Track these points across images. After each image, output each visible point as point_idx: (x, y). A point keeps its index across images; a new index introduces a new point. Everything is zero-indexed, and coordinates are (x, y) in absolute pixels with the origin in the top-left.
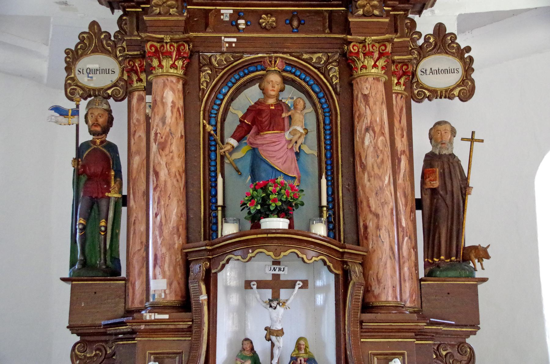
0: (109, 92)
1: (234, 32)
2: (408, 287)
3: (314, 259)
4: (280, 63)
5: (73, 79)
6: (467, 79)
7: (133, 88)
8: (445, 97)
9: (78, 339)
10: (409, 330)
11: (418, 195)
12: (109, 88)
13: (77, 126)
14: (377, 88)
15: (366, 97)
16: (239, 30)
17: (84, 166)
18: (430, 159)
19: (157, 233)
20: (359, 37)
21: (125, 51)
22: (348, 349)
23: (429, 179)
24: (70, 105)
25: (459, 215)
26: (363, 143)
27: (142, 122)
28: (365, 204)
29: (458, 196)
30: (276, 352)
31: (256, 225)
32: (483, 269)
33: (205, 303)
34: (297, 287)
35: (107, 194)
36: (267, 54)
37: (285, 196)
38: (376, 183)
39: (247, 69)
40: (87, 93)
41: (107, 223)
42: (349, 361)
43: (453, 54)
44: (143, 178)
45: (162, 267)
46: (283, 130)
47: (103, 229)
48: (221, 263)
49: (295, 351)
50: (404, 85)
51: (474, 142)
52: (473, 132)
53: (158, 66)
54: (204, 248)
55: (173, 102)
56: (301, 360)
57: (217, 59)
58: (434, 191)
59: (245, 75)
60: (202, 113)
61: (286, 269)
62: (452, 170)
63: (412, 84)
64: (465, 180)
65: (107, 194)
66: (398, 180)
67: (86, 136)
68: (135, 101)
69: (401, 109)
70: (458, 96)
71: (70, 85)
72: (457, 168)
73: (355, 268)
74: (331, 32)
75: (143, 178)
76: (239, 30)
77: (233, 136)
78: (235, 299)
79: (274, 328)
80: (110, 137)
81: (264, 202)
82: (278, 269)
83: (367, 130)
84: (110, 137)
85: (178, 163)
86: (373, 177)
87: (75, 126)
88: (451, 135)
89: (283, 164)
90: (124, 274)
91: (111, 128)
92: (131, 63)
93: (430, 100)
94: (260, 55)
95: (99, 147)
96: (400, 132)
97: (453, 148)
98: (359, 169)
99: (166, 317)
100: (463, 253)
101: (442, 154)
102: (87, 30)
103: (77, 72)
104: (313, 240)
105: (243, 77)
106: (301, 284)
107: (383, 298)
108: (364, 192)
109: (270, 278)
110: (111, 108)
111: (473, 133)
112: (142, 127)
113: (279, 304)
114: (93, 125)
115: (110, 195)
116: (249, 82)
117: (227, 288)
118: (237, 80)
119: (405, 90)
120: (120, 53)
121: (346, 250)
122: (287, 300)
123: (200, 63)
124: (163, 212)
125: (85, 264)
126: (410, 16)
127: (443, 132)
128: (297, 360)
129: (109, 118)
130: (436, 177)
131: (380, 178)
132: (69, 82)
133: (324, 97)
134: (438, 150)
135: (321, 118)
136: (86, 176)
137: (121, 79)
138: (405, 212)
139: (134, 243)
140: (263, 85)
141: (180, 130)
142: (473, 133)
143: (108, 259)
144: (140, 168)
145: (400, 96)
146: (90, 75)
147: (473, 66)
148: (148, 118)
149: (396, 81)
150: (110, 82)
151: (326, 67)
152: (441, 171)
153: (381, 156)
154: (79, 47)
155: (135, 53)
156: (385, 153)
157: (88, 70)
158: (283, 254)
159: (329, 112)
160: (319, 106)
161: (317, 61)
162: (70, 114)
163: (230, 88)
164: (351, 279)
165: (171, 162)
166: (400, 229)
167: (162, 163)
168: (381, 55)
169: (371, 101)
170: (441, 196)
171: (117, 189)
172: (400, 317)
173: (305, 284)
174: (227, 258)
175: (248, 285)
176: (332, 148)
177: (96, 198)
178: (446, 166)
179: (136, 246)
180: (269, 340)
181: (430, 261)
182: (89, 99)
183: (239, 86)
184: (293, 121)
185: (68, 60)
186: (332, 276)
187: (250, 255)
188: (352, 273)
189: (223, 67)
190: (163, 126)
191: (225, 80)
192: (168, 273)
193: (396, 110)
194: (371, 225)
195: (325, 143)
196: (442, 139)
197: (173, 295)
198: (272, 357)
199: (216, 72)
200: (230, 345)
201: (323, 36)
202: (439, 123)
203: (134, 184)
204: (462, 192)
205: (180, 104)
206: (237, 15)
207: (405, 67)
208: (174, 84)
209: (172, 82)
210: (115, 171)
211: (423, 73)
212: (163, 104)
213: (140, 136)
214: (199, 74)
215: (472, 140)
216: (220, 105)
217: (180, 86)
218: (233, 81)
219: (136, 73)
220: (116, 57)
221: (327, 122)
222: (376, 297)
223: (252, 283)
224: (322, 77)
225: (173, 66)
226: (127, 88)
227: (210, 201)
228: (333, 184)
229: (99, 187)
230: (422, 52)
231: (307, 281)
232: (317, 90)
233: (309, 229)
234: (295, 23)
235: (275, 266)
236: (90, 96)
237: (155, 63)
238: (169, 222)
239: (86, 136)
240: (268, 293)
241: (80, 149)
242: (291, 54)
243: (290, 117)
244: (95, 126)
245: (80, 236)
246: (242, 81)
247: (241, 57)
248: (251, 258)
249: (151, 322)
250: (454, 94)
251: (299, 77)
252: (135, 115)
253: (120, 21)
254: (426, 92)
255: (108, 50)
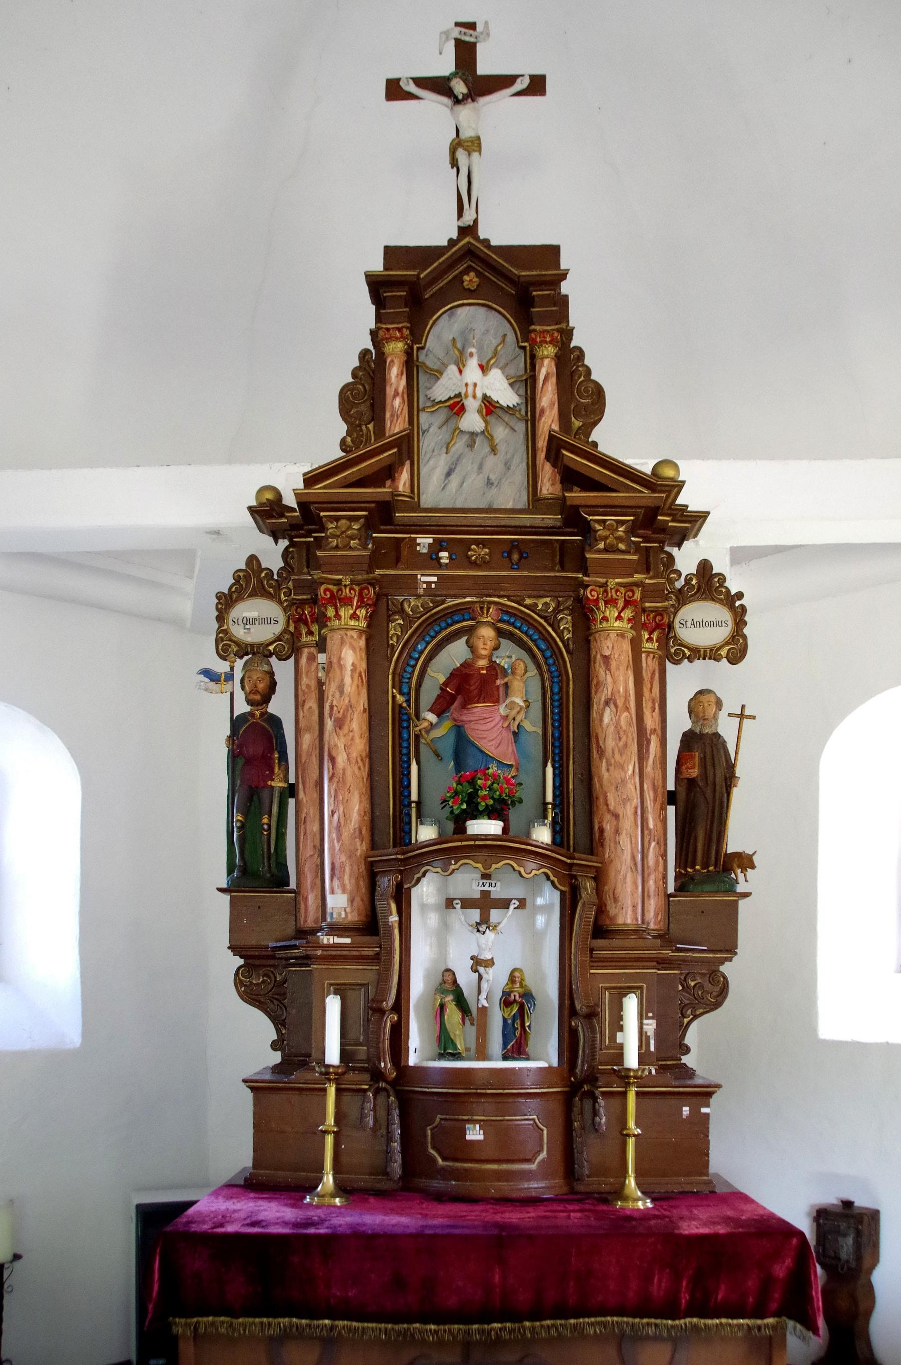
0: (271, 648)
1: (433, 568)
2: (653, 905)
3: (534, 872)
4: (494, 612)
5: (226, 632)
6: (738, 635)
7: (299, 644)
8: (710, 658)
9: (241, 962)
10: (650, 959)
11: (671, 786)
12: (271, 644)
13: (232, 695)
15: (606, 659)
16: (440, 566)
17: (240, 746)
18: (689, 740)
19: (334, 835)
20: (598, 579)
21: (291, 594)
22: (573, 982)
24: (222, 667)
25: (721, 814)
26: (601, 720)
27: (313, 689)
28: (601, 800)
29: (721, 788)
30: (485, 986)
31: (460, 829)
32: (746, 881)
33: (396, 925)
34: (512, 907)
35: (269, 783)
36: (478, 597)
37: (498, 793)
38: (617, 774)
39: (451, 618)
40: (244, 650)
41: (270, 820)
42: (575, 996)
43: (720, 601)
44: (314, 762)
45: (341, 879)
46: (497, 701)
47: (266, 827)
48: (416, 876)
49: (507, 984)
50: (657, 641)
53: (335, 616)
54: (394, 857)
55: (353, 664)
56: (515, 996)
57: (411, 604)
58: (691, 782)
59: (449, 626)
60: (390, 676)
61: (498, 884)
63: (668, 639)
64: (731, 767)
65: (269, 783)
66: (646, 767)
67: (242, 707)
68: (303, 660)
69: (653, 673)
70: (726, 657)
71: (222, 639)
72: (722, 752)
73: (585, 884)
74: (563, 569)
75: (314, 762)
76: (440, 566)
77: (431, 710)
78: (433, 919)
79: (482, 958)
80: (273, 708)
81: (471, 799)
82: (488, 884)
83: (607, 703)
84: (273, 708)
85: (360, 745)
87: (228, 694)
89: (496, 749)
90: (293, 885)
91: (273, 696)
92: (299, 610)
93: (691, 661)
94: (468, 599)
95: (259, 721)
96: (650, 704)
97: (717, 726)
98: (595, 754)
99: (348, 941)
100: (724, 861)
102: (244, 567)
103: (231, 622)
104: (533, 849)
105: (445, 629)
106: (517, 903)
107: (620, 921)
108: (601, 786)
109: (478, 896)
110: (274, 670)
111: (743, 707)
112: (314, 695)
113: (488, 927)
114: (250, 692)
115: (273, 784)
116: (453, 635)
117: (423, 907)
118: (438, 633)
119: (658, 648)
120: (285, 596)
121: (575, 861)
122: (499, 923)
123: (388, 610)
124: (341, 809)
125: (244, 871)
126: (667, 549)
127: (706, 705)
128: (510, 996)
129: (271, 682)
130: (695, 764)
131: (622, 767)
132: (221, 635)
133: (551, 656)
135: (547, 684)
136: (243, 759)
137: (285, 631)
138: (654, 810)
139: (305, 846)
140: (471, 641)
141: (362, 701)
142: (743, 707)
143: (273, 865)
144: (311, 750)
145: (652, 655)
146: (247, 627)
147: (746, 618)
148: (320, 684)
149: (647, 636)
150: (273, 635)
151: (555, 617)
152: (702, 755)
154: (233, 589)
155: (305, 597)
157: (245, 619)
158: (494, 866)
159: (558, 677)
160: (545, 668)
161: (543, 608)
162: (222, 679)
163: (428, 643)
164: (581, 898)
165: (351, 744)
166: (646, 832)
167: (339, 745)
168: (627, 603)
169: (613, 664)
170: (700, 788)
171: (281, 776)
172: (640, 943)
173: (522, 903)
174: (423, 869)
175: (449, 903)
176: (561, 725)
177: (257, 787)
178: (708, 750)
179: (308, 851)
180: (476, 971)
181: (683, 871)
182: (246, 658)
183: (439, 641)
184: (510, 690)
185: (220, 606)
186: (557, 895)
187: (453, 867)
188: (582, 890)
189: (419, 615)
190: (341, 696)
191: (422, 633)
192: (348, 887)
193: (646, 675)
194: (608, 828)
195: (552, 718)
196: (704, 713)
197: (355, 913)
198: (479, 992)
199: (410, 621)
200: (428, 977)
201: (552, 574)
202: (701, 692)
203: (304, 770)
204: (726, 783)
205: (363, 666)
206: (438, 546)
207: (658, 618)
208: (355, 640)
209: (352, 637)
210: (279, 753)
211: (682, 626)
212: (341, 667)
213: (310, 708)
214: (388, 624)
215: (742, 716)
216: (414, 666)
217: (362, 643)
218: (432, 634)
219: (306, 623)
220: (280, 602)
221: (556, 690)
222: (613, 919)
223: (455, 902)
224: (550, 629)
225: (354, 616)
226: (294, 642)
227: (401, 793)
228: (561, 773)
229: (260, 774)
230: (682, 597)
231: (525, 899)
232: (543, 647)
233: (528, 834)
234: (515, 557)
235: (485, 881)
236: (247, 654)
237: (331, 612)
238: (349, 822)
239: (242, 707)
240: (475, 915)
241: (236, 723)
242: (509, 598)
243: (506, 686)
244: (253, 693)
245: (238, 836)
246: (443, 634)
247: (443, 602)
248: (454, 870)
249: (329, 946)
250: (720, 655)
251: (519, 629)
252: (305, 679)
253: (286, 554)
254: (686, 650)
255: (270, 593)
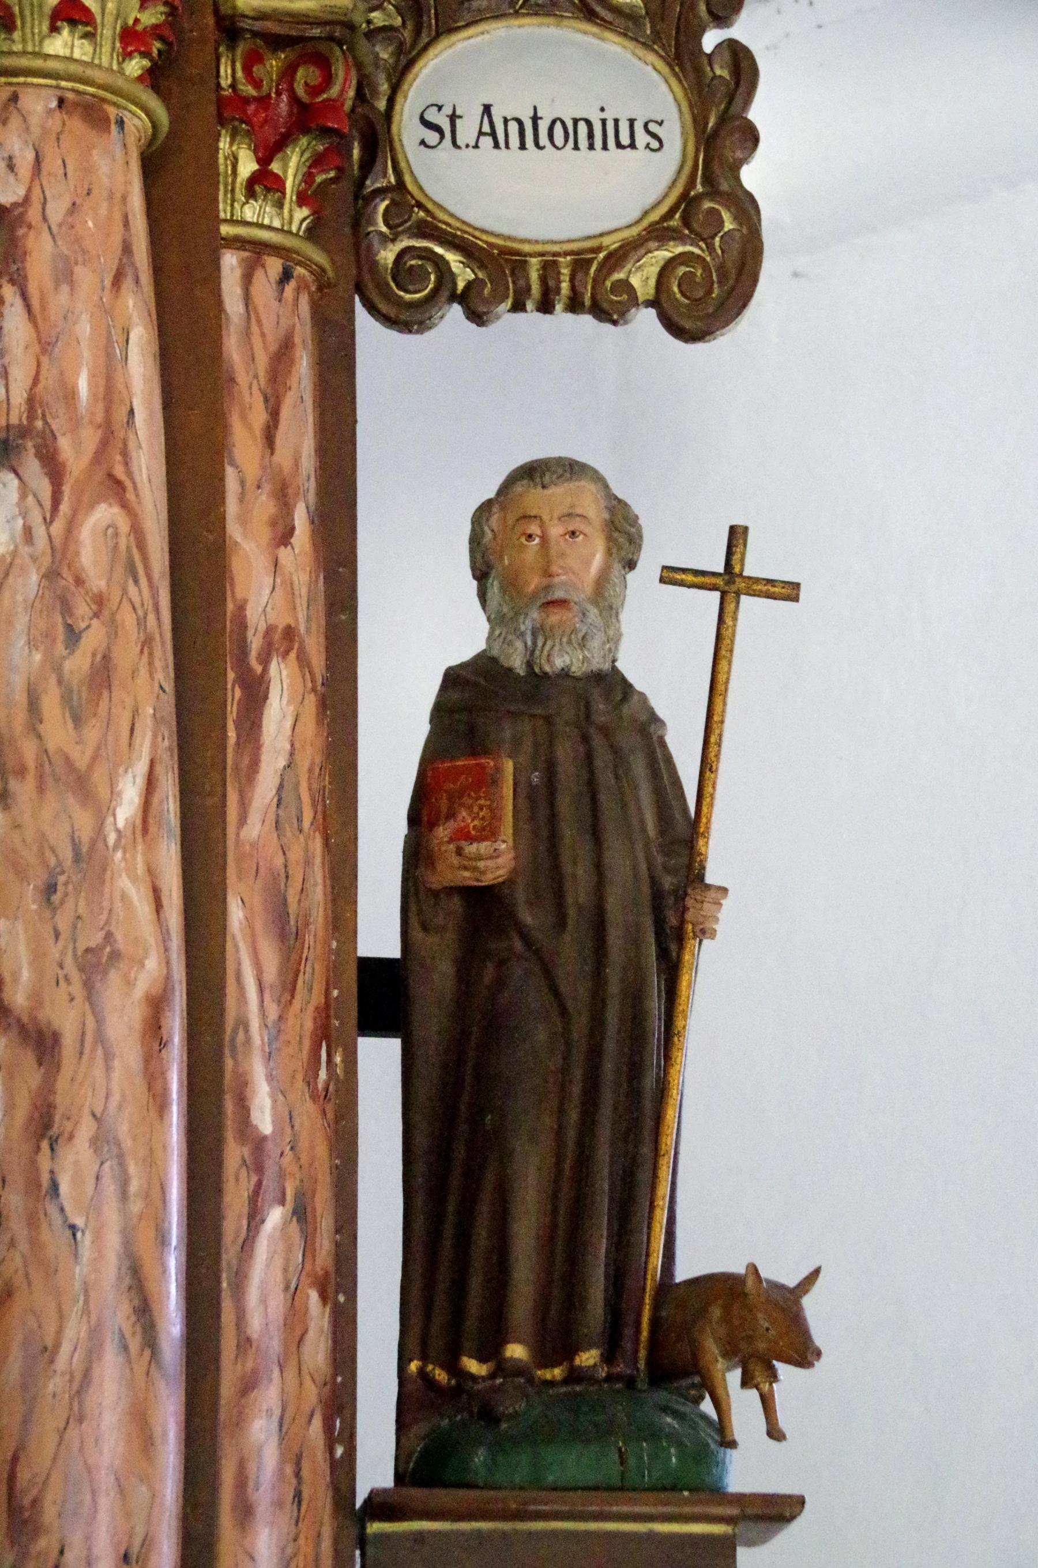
6: (713, 191)
8: (574, 306)
14: (88, 169)
23: (452, 825)
25: (634, 1069)
29: (635, 942)
32: (775, 1433)
50: (302, 199)
51: (738, 594)
52: (733, 530)
62: (606, 779)
66: (243, 820)
70: (653, 303)
72: (639, 768)
86: (30, 781)
88: (609, 552)
93: (477, 317)
96: (264, 505)
100: (656, 1323)
101: (547, 668)
111: (737, 536)
119: (312, 234)
127: (556, 531)
130: (495, 816)
134: (519, 644)
138: (277, 1029)
142: (737, 536)
145: (274, 266)
149: (247, 166)
152: (536, 778)
153: (94, 637)
156: (127, 618)
178: (566, 752)
181: (441, 1376)
196: (547, 573)
207: (305, 76)
211: (432, 137)
250: (625, 286)
254: (453, 259)
